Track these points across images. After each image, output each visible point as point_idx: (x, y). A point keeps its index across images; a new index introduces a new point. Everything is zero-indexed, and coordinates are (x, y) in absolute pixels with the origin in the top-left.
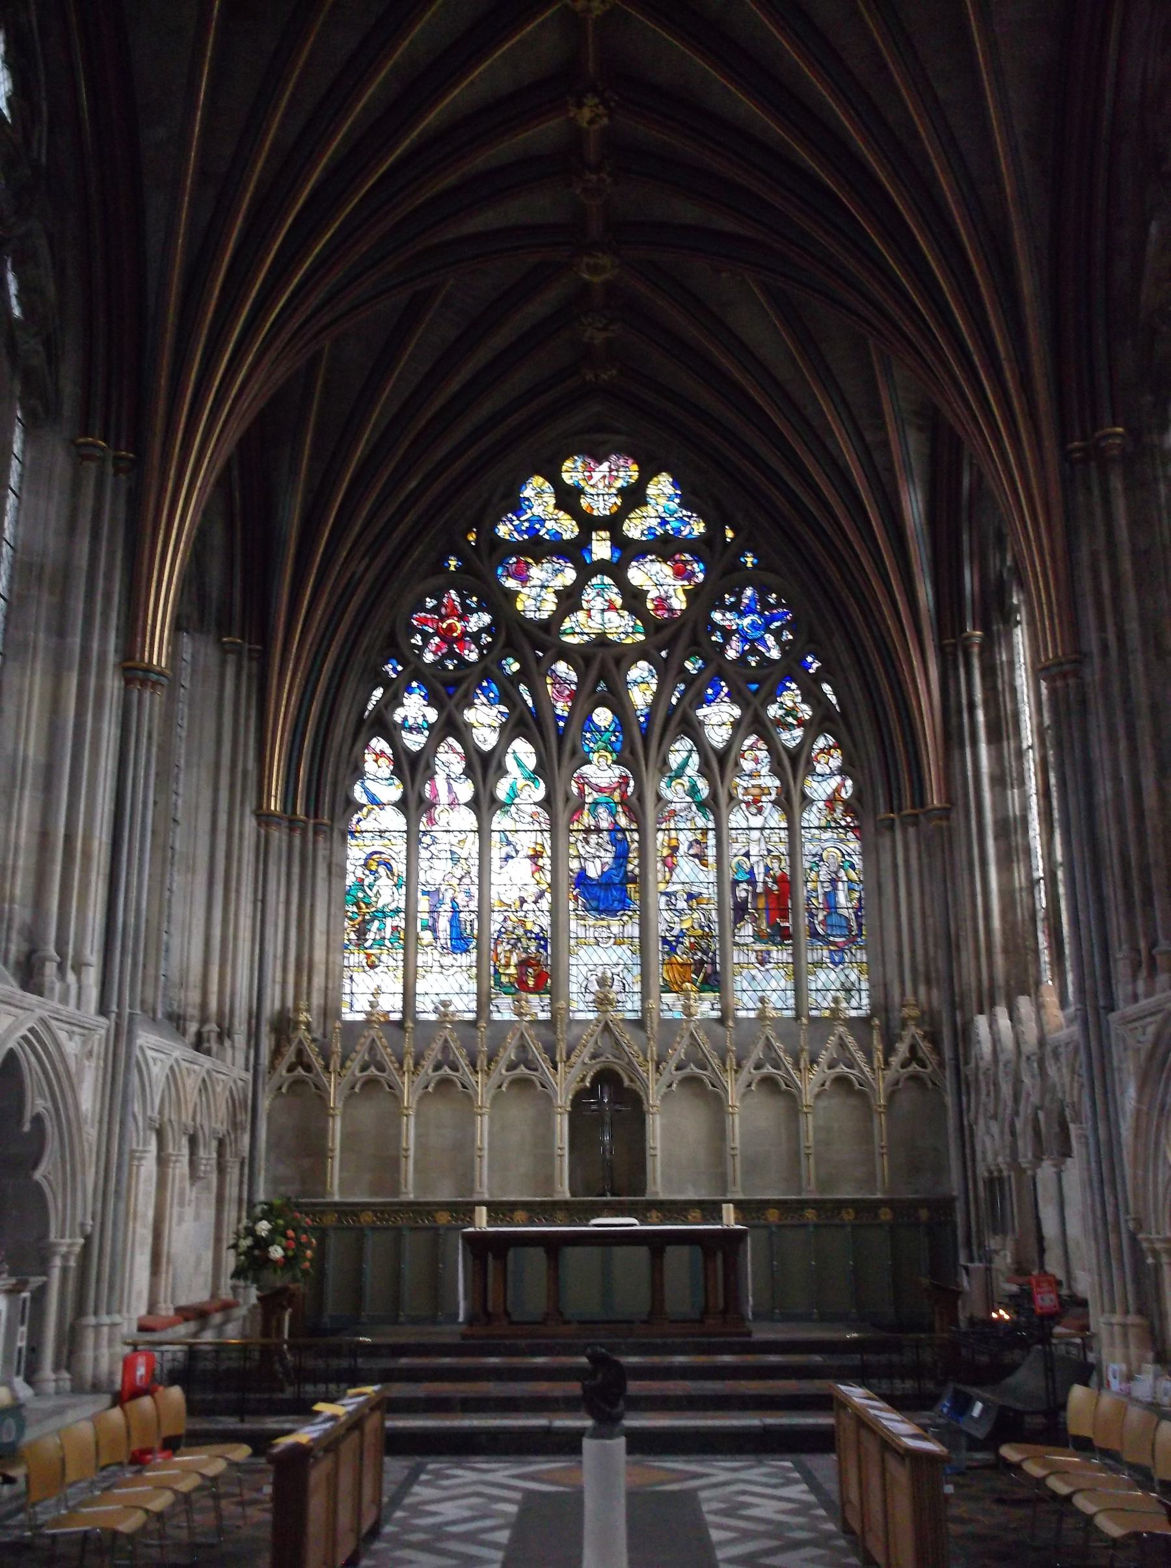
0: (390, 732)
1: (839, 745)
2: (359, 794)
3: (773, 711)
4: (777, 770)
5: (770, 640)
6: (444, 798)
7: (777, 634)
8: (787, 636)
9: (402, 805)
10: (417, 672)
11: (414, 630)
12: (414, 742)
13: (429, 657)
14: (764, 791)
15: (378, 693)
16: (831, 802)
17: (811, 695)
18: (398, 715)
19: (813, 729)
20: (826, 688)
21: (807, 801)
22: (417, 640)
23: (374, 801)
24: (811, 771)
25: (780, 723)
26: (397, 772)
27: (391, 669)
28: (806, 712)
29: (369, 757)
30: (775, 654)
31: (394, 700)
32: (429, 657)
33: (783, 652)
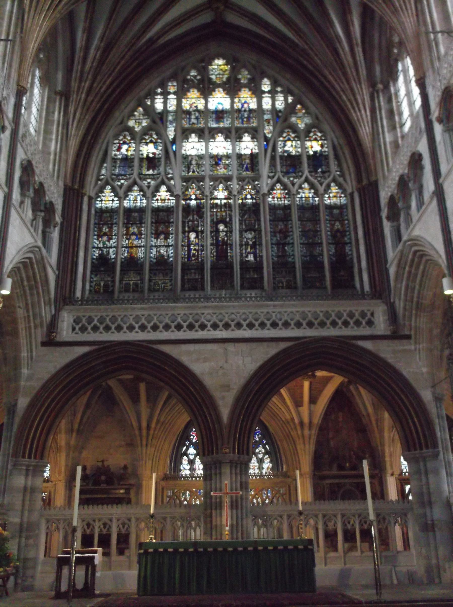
0: (187, 455)
1: (269, 457)
2: (182, 468)
3: (257, 451)
4: (258, 462)
5: (256, 436)
6: (197, 468)
7: (258, 435)
8: (260, 436)
9: (190, 470)
10: (191, 443)
11: (191, 435)
12: (192, 457)
13: (194, 441)
14: (255, 466)
15: (185, 448)
16: (268, 468)
17: (264, 448)
18: (188, 452)
19: (265, 454)
20: (267, 446)
21: (263, 468)
22: (192, 437)
23: (184, 469)
24: (264, 462)
25: (259, 453)
26: (189, 463)
27: (187, 443)
28: (263, 451)
29: (183, 460)
30: (257, 439)
31: (187, 449)
32: (194, 441)
33: (259, 439)
